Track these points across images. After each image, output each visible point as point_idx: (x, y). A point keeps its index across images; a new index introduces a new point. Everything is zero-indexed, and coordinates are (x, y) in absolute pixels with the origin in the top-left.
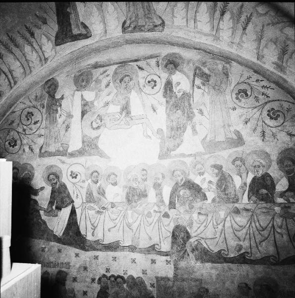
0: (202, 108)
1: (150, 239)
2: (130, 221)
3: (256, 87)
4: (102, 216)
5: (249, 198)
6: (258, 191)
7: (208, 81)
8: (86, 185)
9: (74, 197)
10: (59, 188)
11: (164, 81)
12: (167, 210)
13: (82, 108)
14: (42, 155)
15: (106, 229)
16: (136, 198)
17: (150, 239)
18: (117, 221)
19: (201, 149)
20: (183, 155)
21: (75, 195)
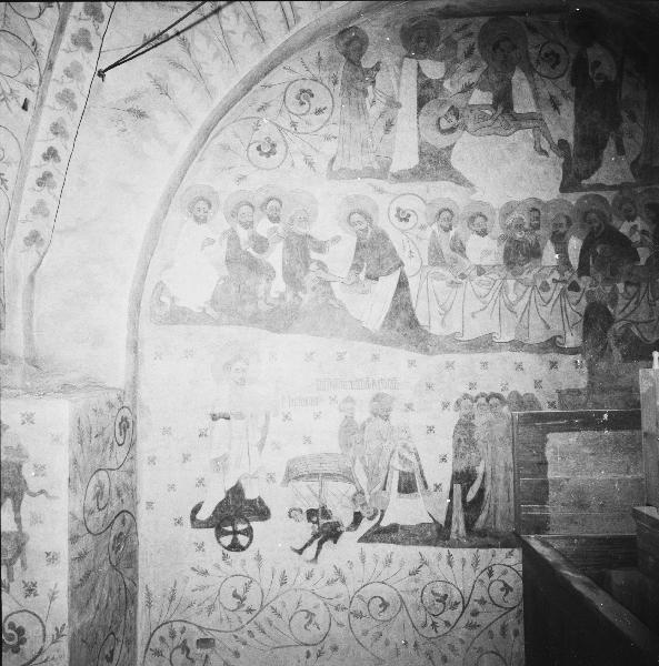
1: (548, 327)
2: (512, 297)
4: (461, 290)
8: (428, 233)
9: (403, 255)
12: (575, 278)
13: (419, 92)
15: (467, 314)
16: (521, 257)
17: (548, 327)
18: (488, 298)
19: (630, 178)
20: (600, 187)
21: (407, 254)
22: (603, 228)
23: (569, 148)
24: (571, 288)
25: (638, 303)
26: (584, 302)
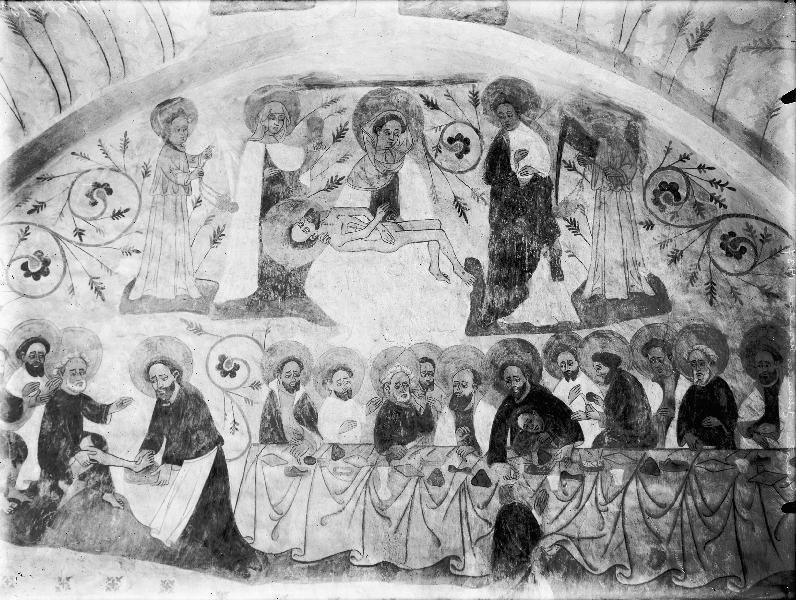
0: (577, 215)
3: (698, 181)
5: (680, 439)
7: (594, 156)
10: (179, 402)
11: (488, 142)
14: (129, 307)
20: (526, 327)
21: (229, 424)
22: (528, 392)
23: (481, 271)
24: (476, 481)
25: (580, 508)
26: (496, 504)
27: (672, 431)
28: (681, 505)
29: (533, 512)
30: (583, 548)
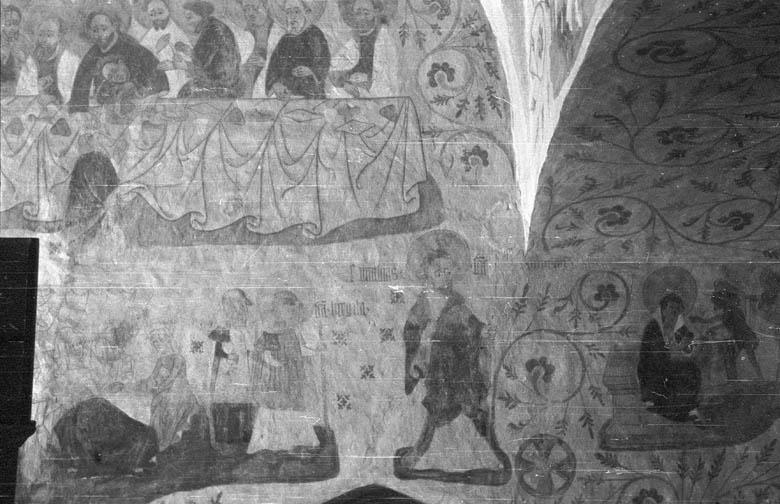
5: (268, 87)
6: (289, 74)
25: (160, 157)
26: (75, 152)
27: (261, 81)
28: (263, 154)
29: (113, 161)
30: (159, 196)
